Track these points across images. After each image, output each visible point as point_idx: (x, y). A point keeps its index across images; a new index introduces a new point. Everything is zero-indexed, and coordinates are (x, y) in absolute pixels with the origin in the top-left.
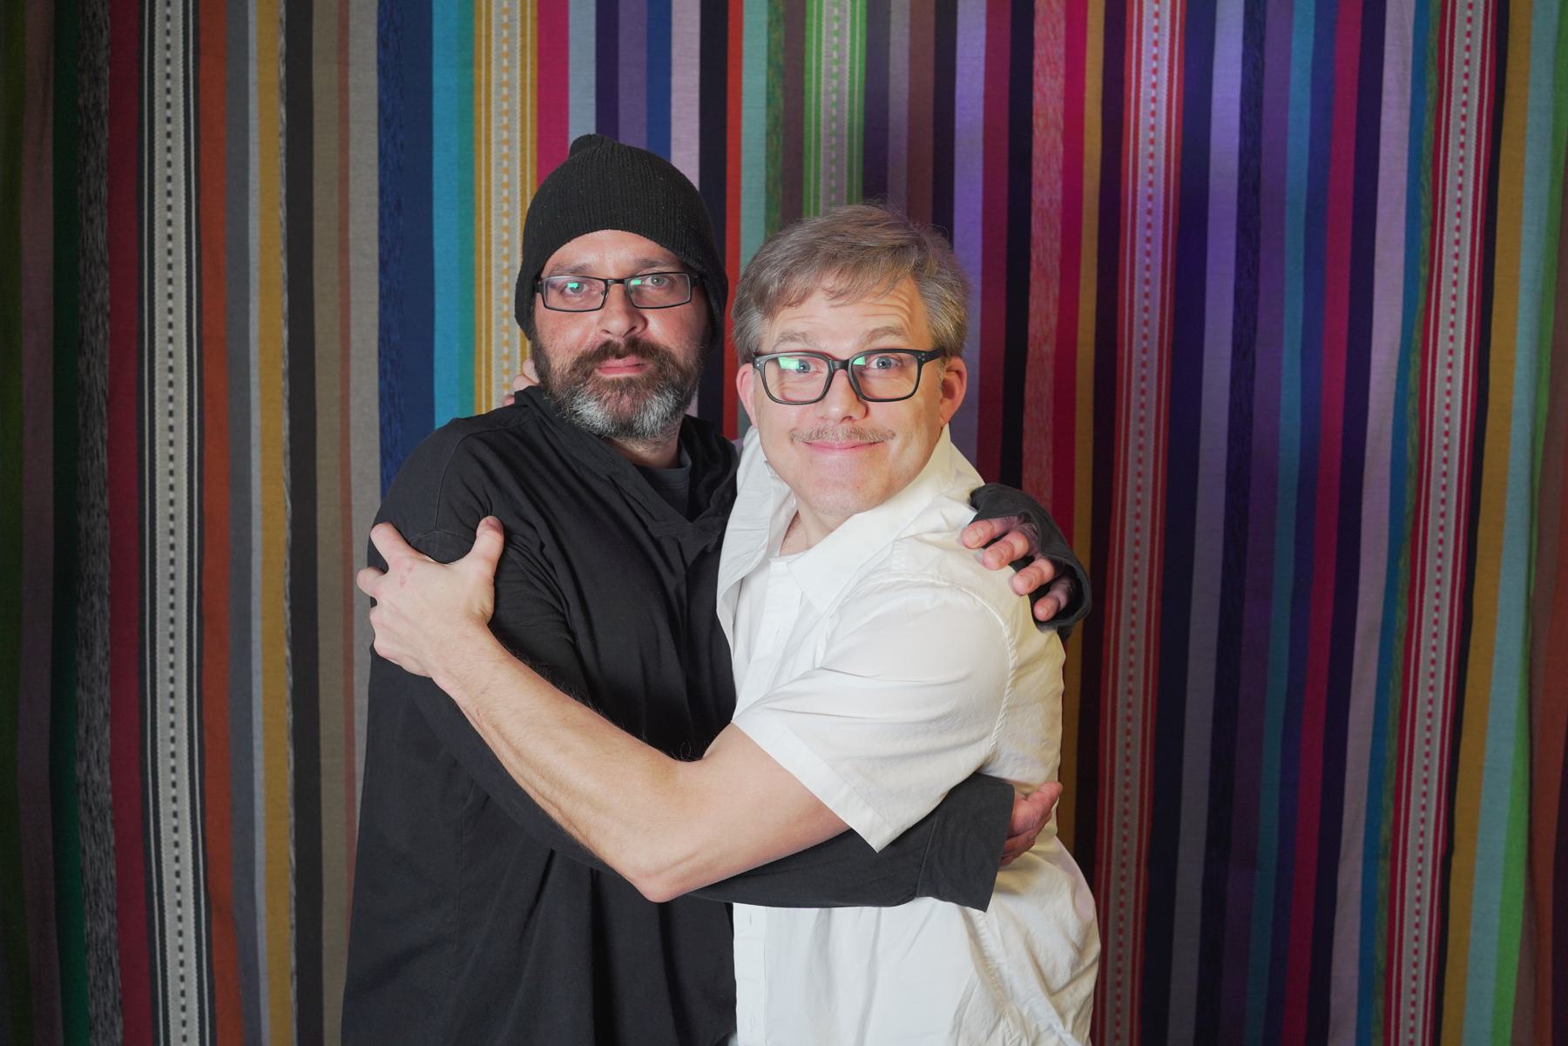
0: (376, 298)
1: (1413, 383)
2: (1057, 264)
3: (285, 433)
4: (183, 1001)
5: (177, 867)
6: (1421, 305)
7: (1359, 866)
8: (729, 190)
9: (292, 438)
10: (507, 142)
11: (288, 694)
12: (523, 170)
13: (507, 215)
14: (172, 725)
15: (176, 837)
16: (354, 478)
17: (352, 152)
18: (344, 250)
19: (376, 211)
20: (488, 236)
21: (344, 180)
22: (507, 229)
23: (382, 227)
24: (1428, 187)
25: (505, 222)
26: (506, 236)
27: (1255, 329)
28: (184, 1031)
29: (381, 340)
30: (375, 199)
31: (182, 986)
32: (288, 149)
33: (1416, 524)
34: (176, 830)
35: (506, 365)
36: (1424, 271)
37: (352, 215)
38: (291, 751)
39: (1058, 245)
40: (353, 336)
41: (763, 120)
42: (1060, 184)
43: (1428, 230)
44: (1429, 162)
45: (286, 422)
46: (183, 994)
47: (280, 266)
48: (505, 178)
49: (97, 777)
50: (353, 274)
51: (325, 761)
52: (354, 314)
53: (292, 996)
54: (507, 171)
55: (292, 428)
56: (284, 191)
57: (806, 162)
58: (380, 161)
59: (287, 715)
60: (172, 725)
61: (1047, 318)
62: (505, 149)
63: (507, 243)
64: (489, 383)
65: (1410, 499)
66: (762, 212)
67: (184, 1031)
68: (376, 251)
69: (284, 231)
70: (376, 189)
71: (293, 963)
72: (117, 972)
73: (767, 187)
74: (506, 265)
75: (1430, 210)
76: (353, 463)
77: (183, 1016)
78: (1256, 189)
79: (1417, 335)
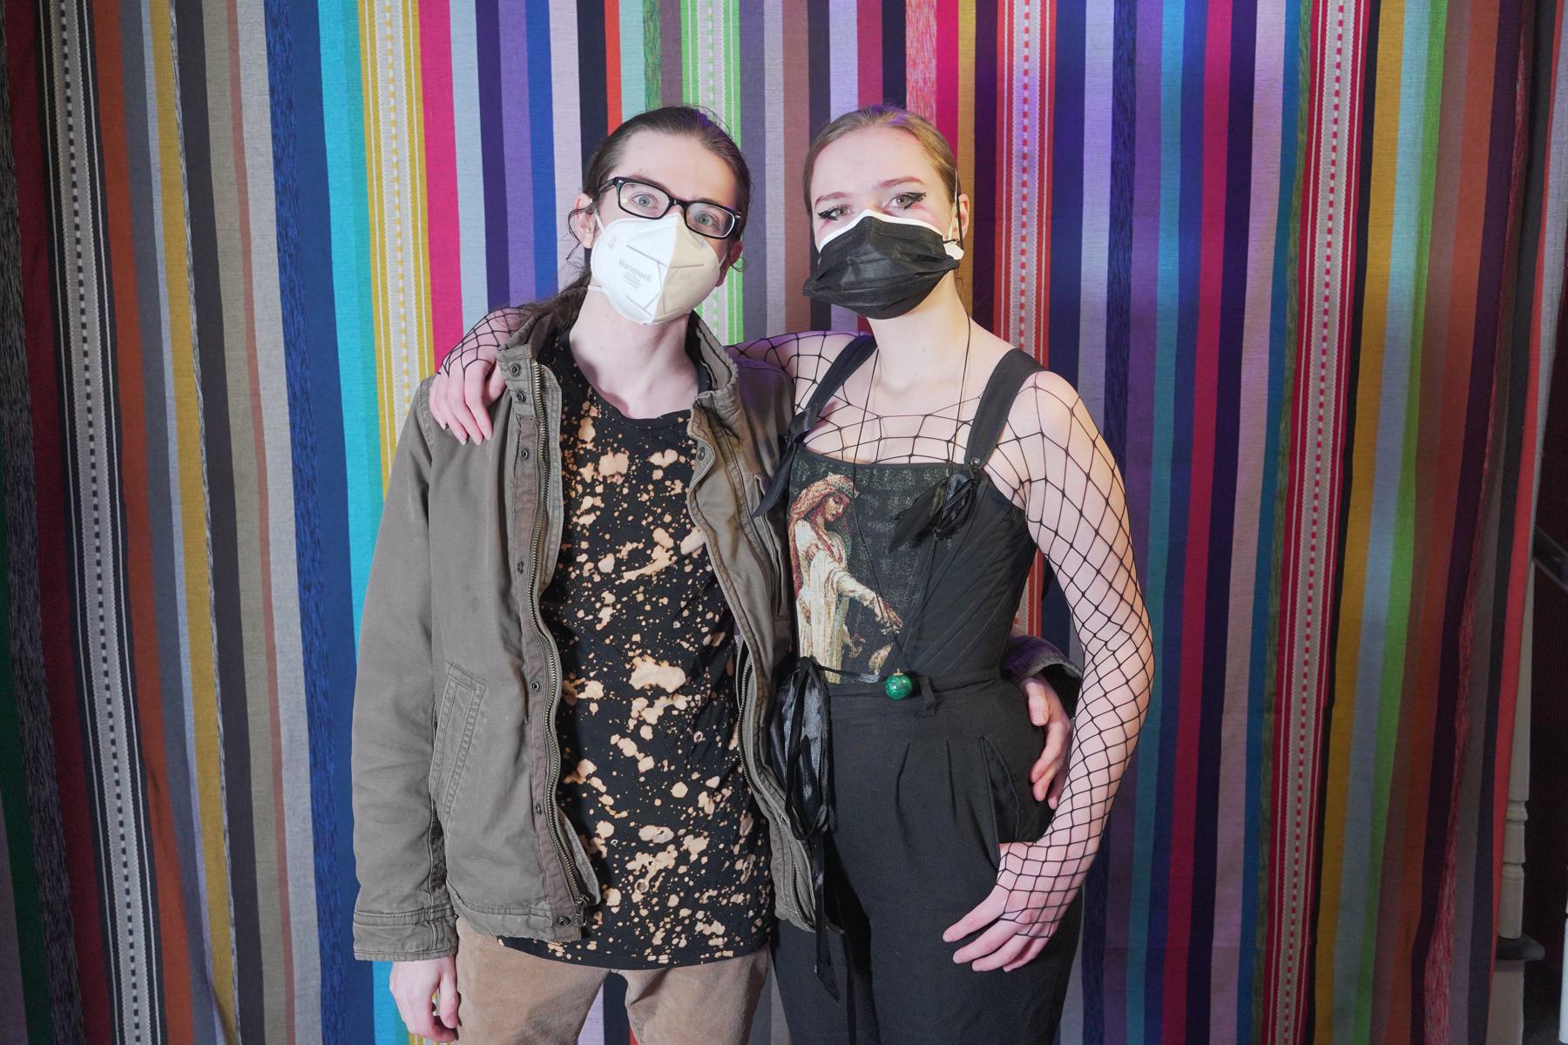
0: (273, 196)
1: (1292, 249)
3: (194, 327)
4: (124, 858)
5: (112, 736)
6: (1300, 172)
7: (1243, 718)
9: (200, 332)
10: (392, 38)
11: (208, 573)
12: (408, 65)
14: (101, 605)
15: (109, 708)
20: (377, 131)
22: (395, 123)
23: (275, 125)
24: (1306, 53)
26: (394, 130)
27: (1132, 199)
28: (127, 885)
29: (279, 235)
30: (267, 98)
31: (123, 844)
32: (180, 52)
33: (1296, 388)
34: (109, 701)
36: (1302, 138)
37: (245, 115)
38: (214, 626)
40: (253, 233)
41: (641, 8)
42: (934, 62)
43: (1307, 95)
44: (1307, 27)
46: (124, 851)
47: (180, 166)
49: (30, 653)
50: (249, 173)
51: (248, 634)
52: (252, 211)
53: (226, 852)
56: (178, 94)
57: (684, 48)
59: (209, 592)
60: (101, 605)
64: (384, 274)
65: (1289, 363)
67: (127, 885)
69: (181, 132)
70: (267, 88)
71: (226, 822)
72: (61, 832)
75: (1308, 75)
76: (259, 355)
77: (125, 871)
78: (1132, 62)
79: (1296, 202)
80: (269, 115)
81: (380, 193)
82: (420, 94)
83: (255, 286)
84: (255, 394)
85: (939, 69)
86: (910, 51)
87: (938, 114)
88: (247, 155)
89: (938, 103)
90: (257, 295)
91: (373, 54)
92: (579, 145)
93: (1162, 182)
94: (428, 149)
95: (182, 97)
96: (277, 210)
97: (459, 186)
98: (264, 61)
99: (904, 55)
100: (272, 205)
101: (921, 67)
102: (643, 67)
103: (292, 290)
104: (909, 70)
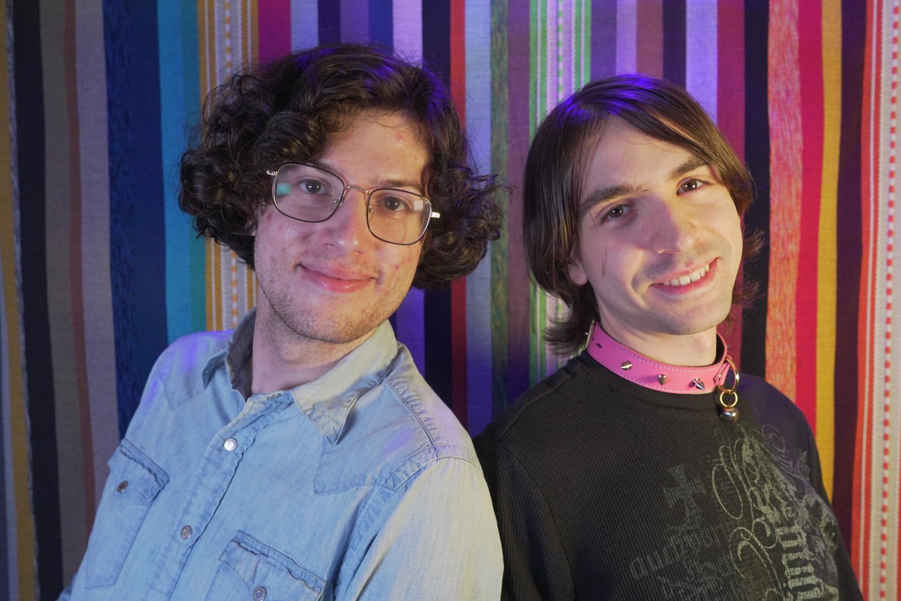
0: (106, 213)
2: (799, 157)
9: (28, 354)
17: (78, 66)
21: (72, 94)
23: (111, 141)
30: (104, 113)
39: (799, 137)
41: (488, 19)
50: (84, 190)
55: (28, 343)
56: (13, 107)
57: (532, 60)
58: (108, 75)
61: (790, 214)
64: (219, 295)
68: (106, 165)
69: (14, 146)
73: (492, 87)
86: (772, 62)
87: (804, 129)
88: (83, 172)
89: (804, 115)
96: (112, 229)
98: (102, 75)
101: (783, 78)
102: (488, 79)
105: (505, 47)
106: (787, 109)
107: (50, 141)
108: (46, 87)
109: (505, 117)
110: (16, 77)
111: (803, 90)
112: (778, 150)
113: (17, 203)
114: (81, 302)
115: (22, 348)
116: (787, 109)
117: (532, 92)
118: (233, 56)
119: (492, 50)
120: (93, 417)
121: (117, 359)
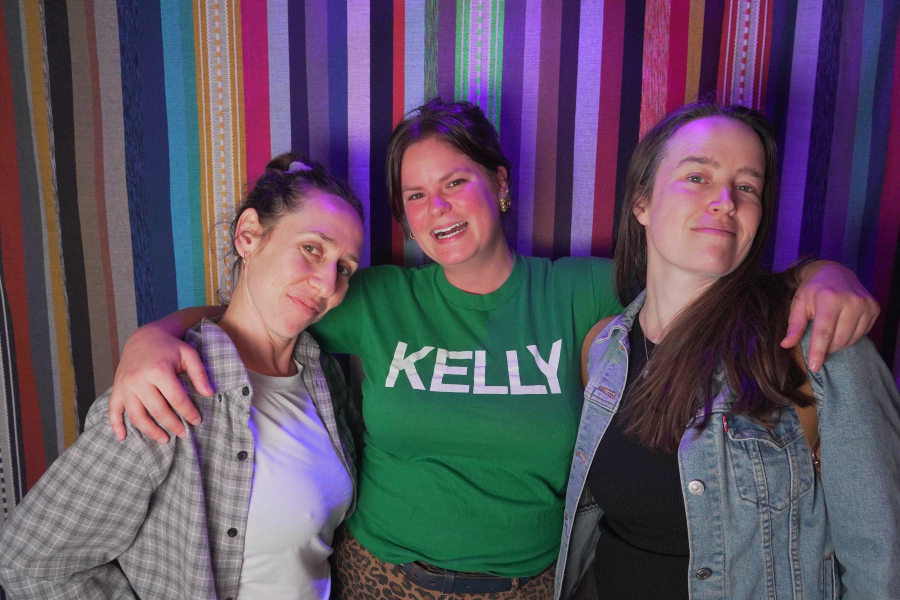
2: (664, 105)
8: (395, 43)
9: (64, 245)
12: (231, 29)
13: (220, 67)
16: (114, 275)
18: (97, 97)
19: (119, 65)
20: (207, 84)
22: (220, 79)
25: (219, 73)
27: (828, 160)
35: (224, 188)
39: (664, 89)
40: (106, 165)
42: (667, 37)
45: (59, 232)
48: (218, 37)
54: (218, 31)
56: (46, 49)
62: (217, 13)
63: (221, 90)
66: (422, 63)
68: (121, 98)
69: (47, 81)
70: (118, 47)
74: (221, 108)
78: (837, 40)
80: (120, 70)
81: (209, 136)
82: (241, 55)
83: (108, 208)
84: (110, 296)
85: (671, 43)
86: (648, 27)
87: (669, 82)
88: (102, 103)
89: (669, 70)
90: (110, 217)
91: (204, 20)
92: (368, 100)
93: (855, 145)
94: (246, 101)
95: (48, 53)
96: (126, 148)
97: (272, 133)
99: (642, 29)
100: (121, 143)
102: (423, 35)
103: (138, 214)
104: (646, 43)
105: (437, 8)
106: (657, 67)
107: (75, 77)
108: (71, 34)
109: (434, 66)
110: (47, 24)
111: (670, 50)
112: (647, 99)
113: (52, 126)
114: (104, 205)
115: (60, 240)
116: (657, 67)
117: (457, 47)
118: (220, 12)
119: (426, 10)
120: (115, 294)
121: (134, 251)
